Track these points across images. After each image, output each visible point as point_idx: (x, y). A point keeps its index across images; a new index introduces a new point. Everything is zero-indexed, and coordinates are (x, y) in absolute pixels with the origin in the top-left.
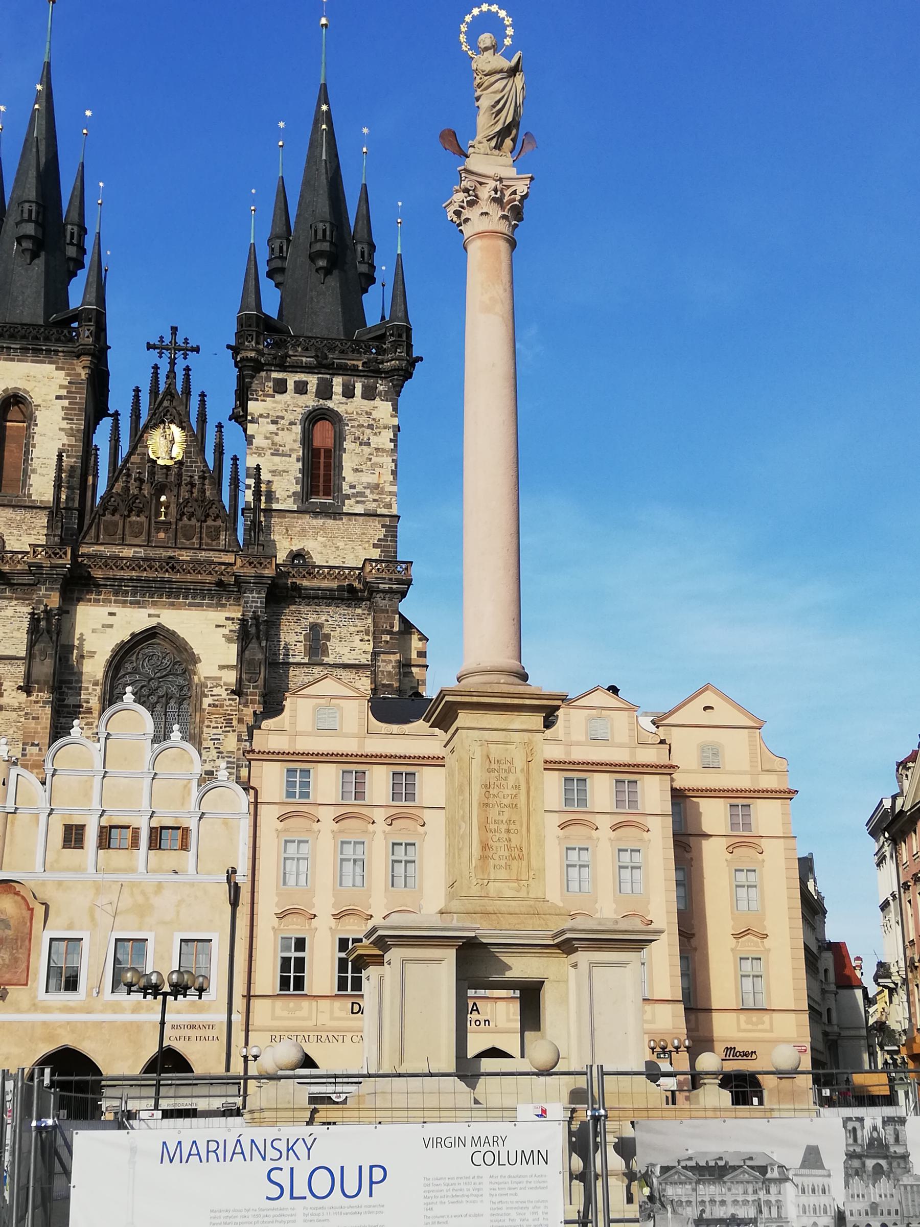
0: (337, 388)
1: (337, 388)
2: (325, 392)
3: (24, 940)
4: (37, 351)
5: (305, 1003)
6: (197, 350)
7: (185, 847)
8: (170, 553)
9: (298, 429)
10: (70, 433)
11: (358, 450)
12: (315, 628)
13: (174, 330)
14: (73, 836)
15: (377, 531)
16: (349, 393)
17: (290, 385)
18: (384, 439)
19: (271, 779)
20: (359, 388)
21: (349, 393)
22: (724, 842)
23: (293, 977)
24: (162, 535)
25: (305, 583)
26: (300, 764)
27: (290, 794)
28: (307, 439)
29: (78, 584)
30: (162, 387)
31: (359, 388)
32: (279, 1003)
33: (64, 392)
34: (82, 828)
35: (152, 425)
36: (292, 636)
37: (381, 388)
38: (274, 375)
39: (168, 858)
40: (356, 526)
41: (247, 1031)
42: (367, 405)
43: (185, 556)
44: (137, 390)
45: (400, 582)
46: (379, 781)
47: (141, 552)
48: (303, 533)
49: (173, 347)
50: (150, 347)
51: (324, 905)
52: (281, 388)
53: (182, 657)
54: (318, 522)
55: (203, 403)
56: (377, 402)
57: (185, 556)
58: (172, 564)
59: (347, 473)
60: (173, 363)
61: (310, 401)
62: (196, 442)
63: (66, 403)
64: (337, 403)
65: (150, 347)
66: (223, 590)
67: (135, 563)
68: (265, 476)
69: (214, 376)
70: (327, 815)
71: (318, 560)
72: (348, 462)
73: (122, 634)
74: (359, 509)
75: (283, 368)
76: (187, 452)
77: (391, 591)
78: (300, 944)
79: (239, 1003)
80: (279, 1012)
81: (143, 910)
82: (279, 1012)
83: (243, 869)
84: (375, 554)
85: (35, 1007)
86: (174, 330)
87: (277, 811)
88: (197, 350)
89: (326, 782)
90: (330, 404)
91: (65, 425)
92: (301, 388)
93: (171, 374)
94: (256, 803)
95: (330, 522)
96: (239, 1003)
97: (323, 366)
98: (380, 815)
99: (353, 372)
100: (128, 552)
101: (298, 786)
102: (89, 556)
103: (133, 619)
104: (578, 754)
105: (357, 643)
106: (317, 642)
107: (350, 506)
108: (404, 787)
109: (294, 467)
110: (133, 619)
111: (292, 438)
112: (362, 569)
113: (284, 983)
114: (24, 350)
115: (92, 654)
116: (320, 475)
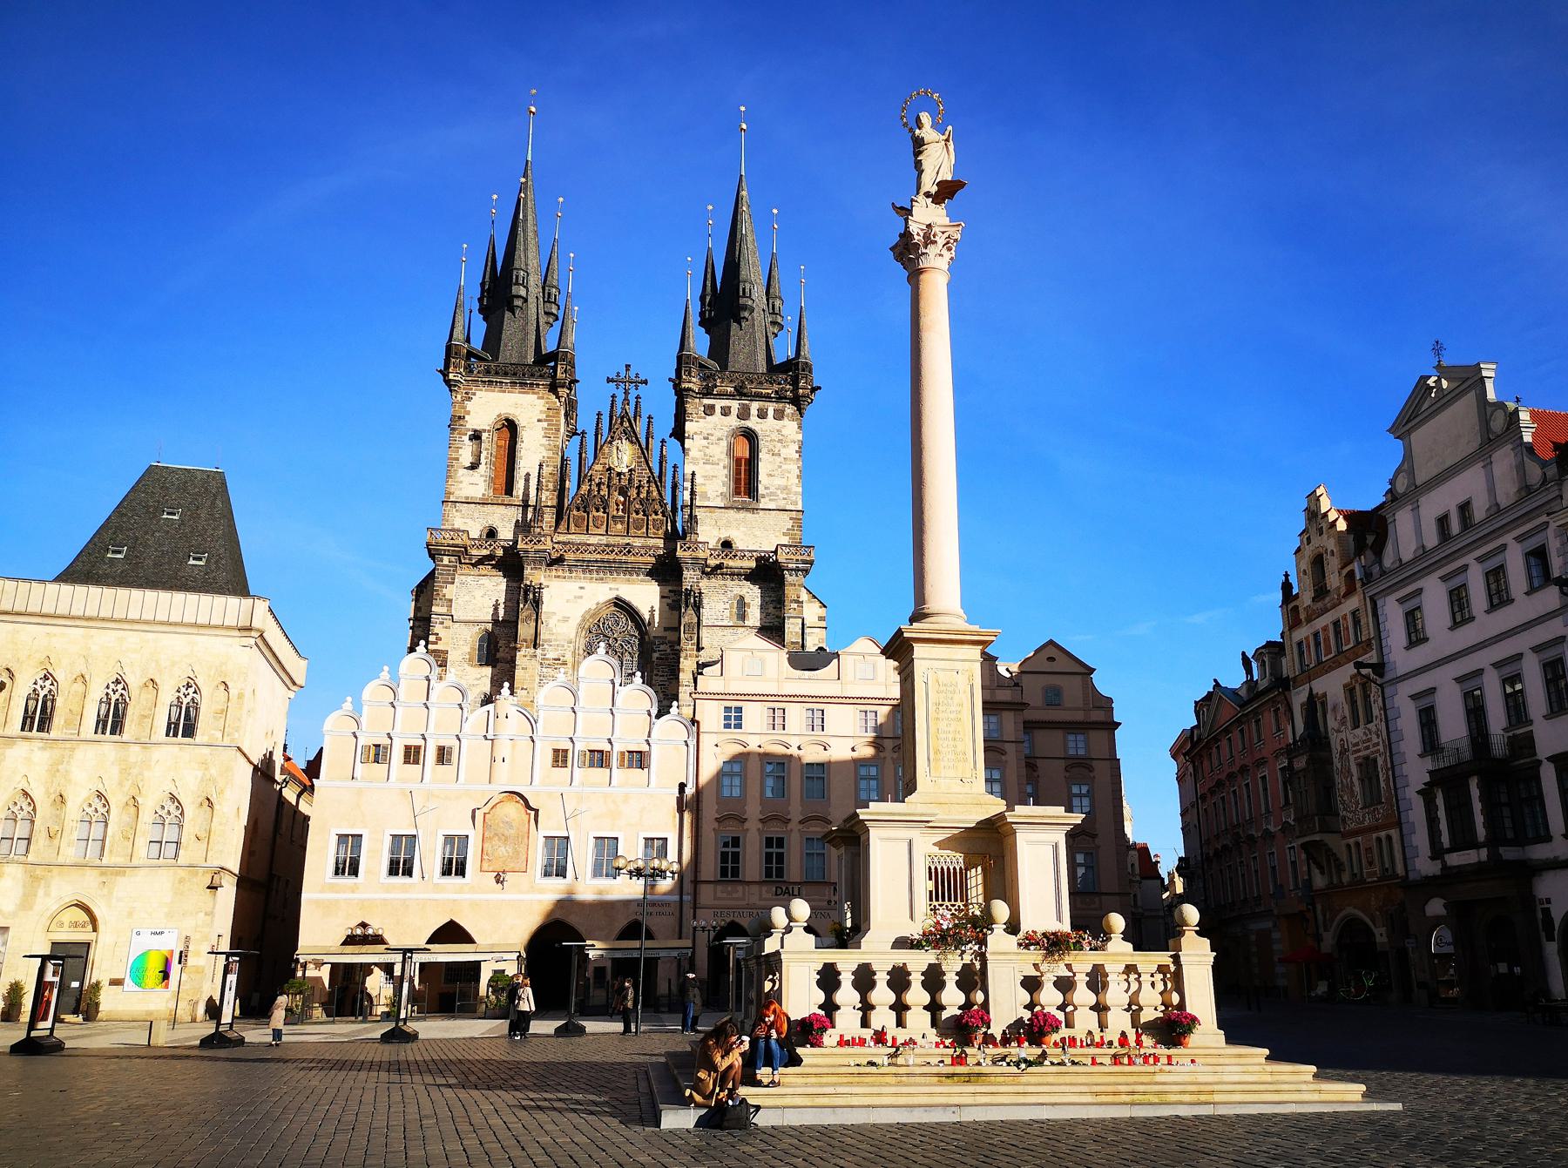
2: (744, 414)
4: (523, 385)
5: (740, 888)
6: (646, 382)
8: (627, 540)
9: (724, 444)
11: (771, 458)
13: (628, 367)
14: (560, 758)
15: (785, 522)
17: (718, 410)
18: (791, 451)
20: (771, 413)
22: (1062, 763)
24: (619, 526)
25: (731, 563)
27: (727, 726)
30: (618, 411)
32: (719, 888)
33: (543, 416)
38: (706, 401)
41: (695, 908)
43: (637, 542)
44: (599, 414)
45: (805, 562)
47: (604, 540)
48: (728, 525)
49: (627, 381)
50: (609, 380)
52: (709, 410)
54: (742, 514)
56: (786, 421)
57: (637, 542)
58: (628, 549)
60: (626, 392)
61: (733, 421)
62: (644, 452)
63: (545, 424)
64: (753, 423)
65: (609, 380)
67: (600, 548)
68: (698, 480)
69: (658, 403)
71: (739, 544)
77: (797, 570)
78: (736, 842)
80: (719, 895)
82: (719, 895)
84: (785, 540)
86: (628, 367)
88: (646, 382)
91: (544, 441)
92: (726, 412)
95: (749, 515)
97: (740, 393)
99: (767, 398)
100: (593, 540)
102: (564, 543)
111: (719, 451)
112: (775, 552)
113: (724, 872)
114: (513, 384)
115: (566, 620)
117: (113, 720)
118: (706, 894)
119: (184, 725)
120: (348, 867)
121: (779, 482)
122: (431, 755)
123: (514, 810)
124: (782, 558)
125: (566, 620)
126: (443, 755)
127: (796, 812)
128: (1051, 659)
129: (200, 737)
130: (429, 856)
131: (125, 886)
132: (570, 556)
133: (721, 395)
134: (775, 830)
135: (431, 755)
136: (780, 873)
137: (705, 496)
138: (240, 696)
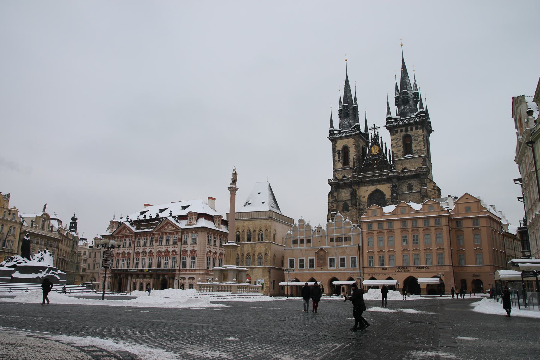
0: (409, 129)
1: (409, 129)
2: (407, 131)
3: (325, 259)
7: (350, 240)
9: (402, 140)
10: (356, 152)
12: (410, 184)
14: (332, 240)
16: (412, 130)
17: (399, 131)
18: (421, 138)
20: (414, 128)
21: (412, 130)
26: (370, 224)
28: (404, 142)
29: (360, 183)
31: (414, 128)
34: (333, 238)
37: (419, 127)
39: (348, 242)
40: (416, 160)
42: (416, 131)
48: (405, 164)
49: (375, 128)
51: (376, 250)
52: (397, 132)
53: (382, 194)
55: (381, 139)
56: (419, 130)
59: (414, 148)
60: (375, 132)
61: (404, 133)
64: (410, 133)
66: (388, 180)
70: (375, 232)
72: (413, 146)
73: (370, 192)
79: (361, 269)
81: (344, 253)
83: (360, 245)
85: (328, 270)
87: (366, 233)
89: (375, 227)
92: (401, 131)
93: (375, 134)
94: (362, 232)
96: (361, 269)
103: (372, 188)
105: (419, 186)
106: (410, 188)
109: (401, 149)
110: (372, 188)
115: (364, 197)
117: (249, 239)
118: (366, 271)
119: (261, 239)
120: (292, 265)
121: (418, 148)
122: (305, 241)
123: (322, 253)
124: (418, 171)
125: (364, 197)
126: (309, 241)
127: (386, 250)
128: (467, 198)
130: (307, 263)
131: (255, 271)
134: (381, 254)
135: (305, 241)
137: (397, 157)
138: (270, 232)
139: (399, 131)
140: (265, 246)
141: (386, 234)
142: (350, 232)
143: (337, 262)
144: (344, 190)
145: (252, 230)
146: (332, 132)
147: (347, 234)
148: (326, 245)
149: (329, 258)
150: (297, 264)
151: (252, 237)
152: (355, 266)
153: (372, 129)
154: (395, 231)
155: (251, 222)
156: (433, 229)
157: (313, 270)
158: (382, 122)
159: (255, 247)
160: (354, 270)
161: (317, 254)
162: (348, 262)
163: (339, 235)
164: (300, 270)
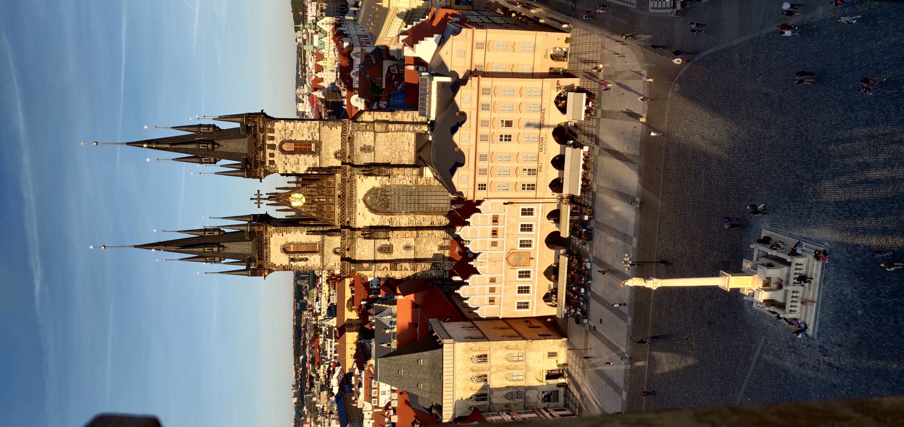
0: (271, 142)
1: (271, 142)
2: (273, 147)
9: (288, 156)
14: (494, 244)
15: (325, 129)
16: (272, 138)
17: (271, 159)
19: (480, 195)
20: (270, 135)
21: (272, 138)
23: (532, 187)
31: (270, 135)
35: (289, 203)
36: (366, 158)
38: (267, 164)
39: (500, 220)
40: (324, 136)
46: (481, 165)
48: (328, 154)
49: (258, 199)
52: (272, 162)
53: (373, 192)
56: (275, 128)
59: (304, 139)
61: (277, 152)
64: (277, 143)
72: (300, 138)
74: (318, 134)
75: (264, 163)
76: (300, 193)
79: (537, 201)
81: (514, 226)
90: (277, 145)
92: (272, 155)
93: (268, 199)
96: (537, 201)
97: (262, 149)
98: (491, 165)
100: (338, 210)
101: (483, 187)
103: (361, 207)
104: (475, 106)
106: (367, 149)
107: (317, 138)
108: (484, 158)
109: (303, 157)
110: (361, 207)
111: (292, 158)
113: (533, 189)
115: (373, 219)
116: (302, 148)
120: (525, 306)
121: (305, 132)
123: (511, 259)
125: (373, 219)
129: (487, 353)
130: (524, 282)
132: (348, 219)
133: (264, 157)
136: (534, 170)
139: (271, 159)
140: (496, 350)
141: (494, 164)
142: (486, 217)
143: (526, 236)
144: (357, 252)
145: (471, 374)
146: (255, 273)
147: (490, 221)
148: (500, 252)
149: (519, 248)
150: (524, 298)
151: (482, 373)
152: (532, 209)
153: (259, 204)
154: (491, 151)
155: (458, 377)
156: (494, 99)
157: (535, 271)
158: (250, 185)
159: (496, 366)
160: (538, 212)
161: (513, 266)
162: (527, 220)
163: (490, 232)
164: (534, 292)
